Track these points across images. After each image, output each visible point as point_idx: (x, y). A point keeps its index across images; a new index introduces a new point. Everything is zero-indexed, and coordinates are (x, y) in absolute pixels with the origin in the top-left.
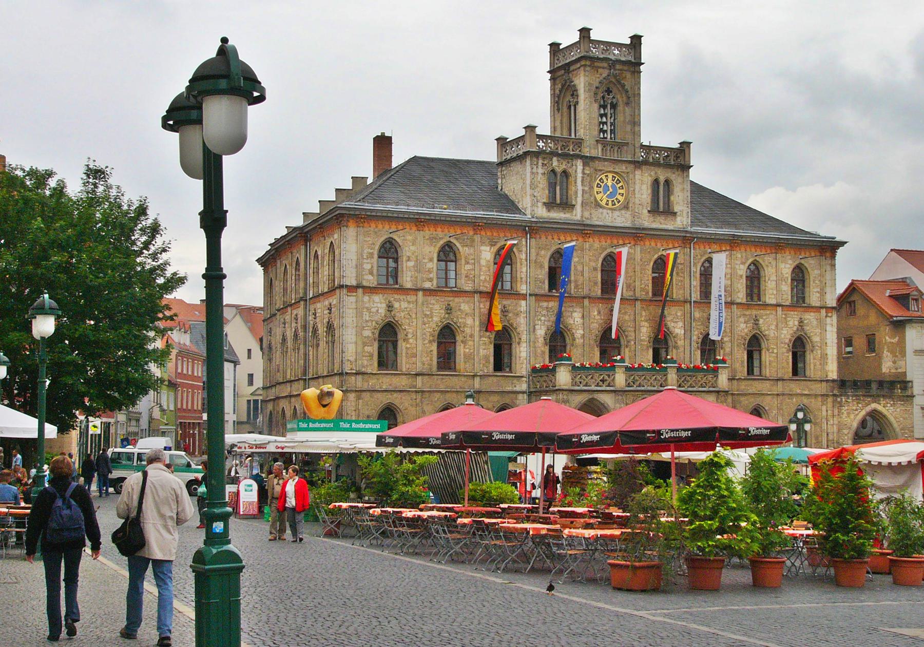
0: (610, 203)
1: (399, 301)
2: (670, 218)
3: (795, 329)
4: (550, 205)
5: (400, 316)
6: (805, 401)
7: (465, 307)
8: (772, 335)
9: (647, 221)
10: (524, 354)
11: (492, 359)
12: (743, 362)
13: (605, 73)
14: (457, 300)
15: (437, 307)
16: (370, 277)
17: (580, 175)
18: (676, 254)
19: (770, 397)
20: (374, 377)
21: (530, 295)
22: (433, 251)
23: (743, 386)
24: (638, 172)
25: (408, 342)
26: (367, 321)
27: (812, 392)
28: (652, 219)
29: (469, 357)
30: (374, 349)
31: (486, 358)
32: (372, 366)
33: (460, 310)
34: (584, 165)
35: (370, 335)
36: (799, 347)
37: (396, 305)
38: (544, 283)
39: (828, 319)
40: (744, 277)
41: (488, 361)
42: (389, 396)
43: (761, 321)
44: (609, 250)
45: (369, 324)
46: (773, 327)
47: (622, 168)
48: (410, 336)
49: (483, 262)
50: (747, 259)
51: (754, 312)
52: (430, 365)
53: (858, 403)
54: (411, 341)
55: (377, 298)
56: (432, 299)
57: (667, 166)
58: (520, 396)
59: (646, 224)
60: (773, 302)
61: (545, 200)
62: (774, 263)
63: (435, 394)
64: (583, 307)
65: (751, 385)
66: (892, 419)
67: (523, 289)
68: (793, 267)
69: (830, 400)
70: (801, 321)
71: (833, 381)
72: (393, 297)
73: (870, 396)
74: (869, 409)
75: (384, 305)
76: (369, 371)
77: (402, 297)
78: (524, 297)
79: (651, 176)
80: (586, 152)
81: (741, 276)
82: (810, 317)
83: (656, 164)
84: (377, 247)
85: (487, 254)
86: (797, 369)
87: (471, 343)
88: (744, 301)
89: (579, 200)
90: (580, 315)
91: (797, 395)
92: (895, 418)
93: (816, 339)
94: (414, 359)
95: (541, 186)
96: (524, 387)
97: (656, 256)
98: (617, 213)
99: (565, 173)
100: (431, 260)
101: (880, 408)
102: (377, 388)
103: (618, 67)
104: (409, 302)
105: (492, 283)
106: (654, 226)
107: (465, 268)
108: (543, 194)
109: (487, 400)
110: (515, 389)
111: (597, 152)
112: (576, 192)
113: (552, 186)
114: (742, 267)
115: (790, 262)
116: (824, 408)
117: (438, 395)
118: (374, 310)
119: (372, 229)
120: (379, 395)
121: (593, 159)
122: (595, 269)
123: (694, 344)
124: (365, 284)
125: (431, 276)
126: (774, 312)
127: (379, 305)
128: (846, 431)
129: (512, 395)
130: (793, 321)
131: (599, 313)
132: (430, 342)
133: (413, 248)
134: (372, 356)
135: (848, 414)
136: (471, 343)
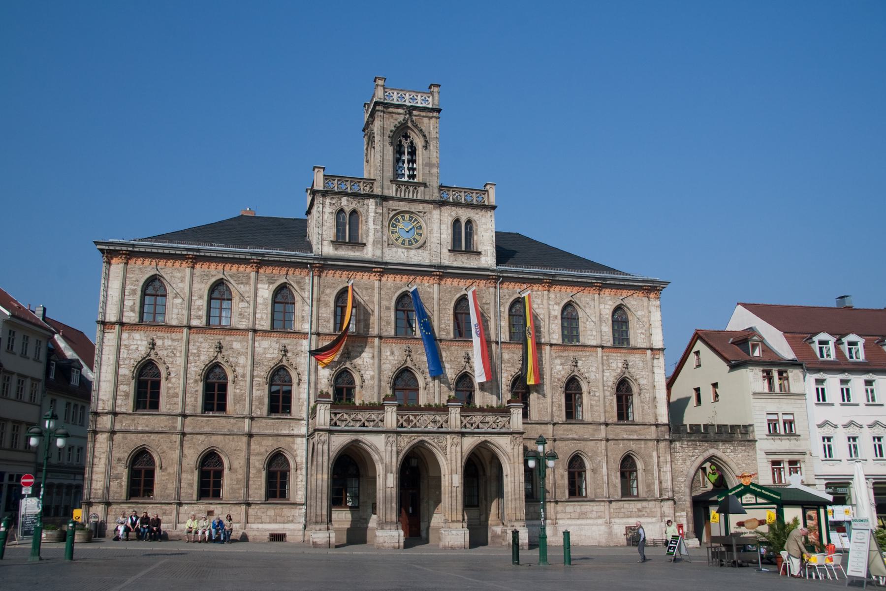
0: (407, 242)
1: (163, 338)
2: (474, 256)
3: (619, 371)
4: (337, 242)
6: (633, 446)
7: (236, 345)
8: (592, 376)
9: (448, 259)
10: (304, 396)
11: (266, 401)
12: (560, 406)
13: (401, 118)
14: (228, 338)
15: (205, 345)
16: (132, 314)
17: (372, 214)
18: (474, 292)
19: (593, 443)
20: (129, 417)
21: (312, 334)
22: (202, 288)
23: (561, 431)
24: (436, 213)
25: (170, 382)
26: (124, 359)
27: (640, 437)
28: (452, 258)
29: (238, 399)
30: (128, 388)
31: (260, 399)
32: (126, 405)
33: (231, 348)
34: (376, 204)
36: (623, 391)
37: (159, 343)
38: (328, 321)
39: (655, 361)
40: (559, 317)
41: (261, 402)
42: (145, 437)
43: (580, 363)
44: (404, 289)
45: (127, 362)
46: (594, 369)
47: (420, 207)
48: (173, 375)
49: (260, 300)
50: (562, 299)
51: (572, 354)
52: (195, 406)
53: (695, 448)
54: (173, 380)
55: (137, 335)
56: (199, 338)
57: (469, 205)
58: (299, 440)
59: (446, 263)
60: (594, 343)
61: (332, 239)
62: (591, 303)
63: (198, 436)
64: (373, 347)
65: (571, 430)
66: (733, 465)
67: (306, 327)
68: (613, 307)
69: (662, 445)
70: (626, 365)
71: (664, 425)
72: (153, 335)
73: (707, 441)
74: (707, 455)
75: (145, 343)
76: (124, 410)
77: (166, 335)
78: (304, 335)
79: (451, 216)
80: (377, 191)
81: (556, 317)
82: (635, 359)
83: (457, 204)
84: (141, 284)
85: (265, 292)
86: (623, 412)
87: (241, 383)
88: (560, 342)
89: (371, 239)
90: (370, 355)
91: (623, 440)
92: (738, 464)
93: (642, 382)
94: (175, 399)
95: (328, 225)
96: (303, 430)
97: (458, 296)
98: (413, 252)
99: (354, 212)
100: (201, 297)
101: (719, 453)
102: (132, 428)
103: (415, 113)
104: (173, 340)
105: (269, 321)
106: (455, 264)
107: (237, 305)
108: (330, 232)
109: (260, 444)
110: (292, 432)
111: (391, 191)
112: (368, 231)
113: (339, 226)
114: (556, 307)
115: (610, 303)
116: (655, 454)
117: (203, 437)
118: (133, 347)
119: (137, 266)
120: (133, 436)
121: (385, 198)
122: (388, 308)
123: (504, 387)
124: (125, 320)
125: (200, 313)
126: (594, 354)
127: (139, 343)
128: (682, 479)
129: (290, 439)
130: (616, 362)
131: (392, 353)
132: (196, 381)
133: (181, 285)
134: (127, 395)
135: (684, 461)
136: (241, 383)
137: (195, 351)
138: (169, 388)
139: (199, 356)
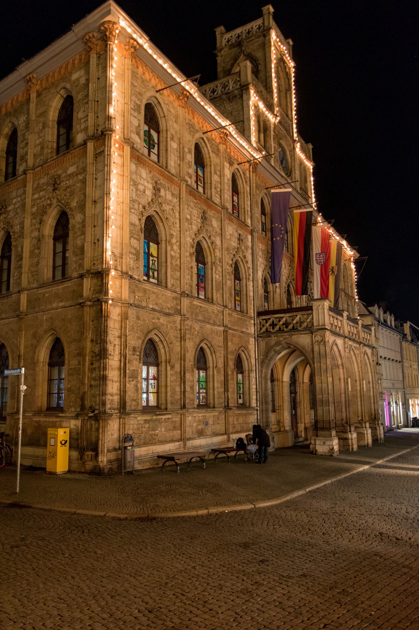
5: (166, 207)
25: (172, 249)
33: (212, 225)
35: (137, 222)
54: (175, 247)
75: (150, 186)
102: (144, 304)
104: (173, 195)
127: (146, 184)
137: (189, 217)
138: (172, 257)
139: (191, 224)
